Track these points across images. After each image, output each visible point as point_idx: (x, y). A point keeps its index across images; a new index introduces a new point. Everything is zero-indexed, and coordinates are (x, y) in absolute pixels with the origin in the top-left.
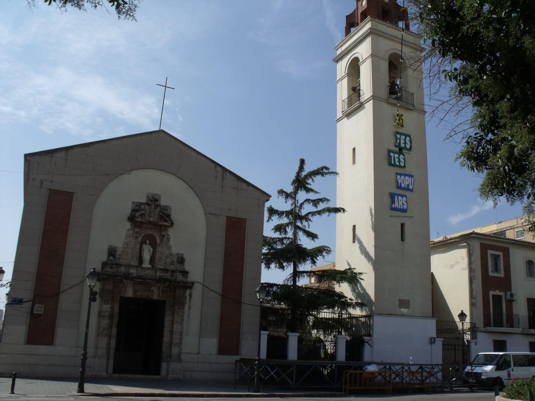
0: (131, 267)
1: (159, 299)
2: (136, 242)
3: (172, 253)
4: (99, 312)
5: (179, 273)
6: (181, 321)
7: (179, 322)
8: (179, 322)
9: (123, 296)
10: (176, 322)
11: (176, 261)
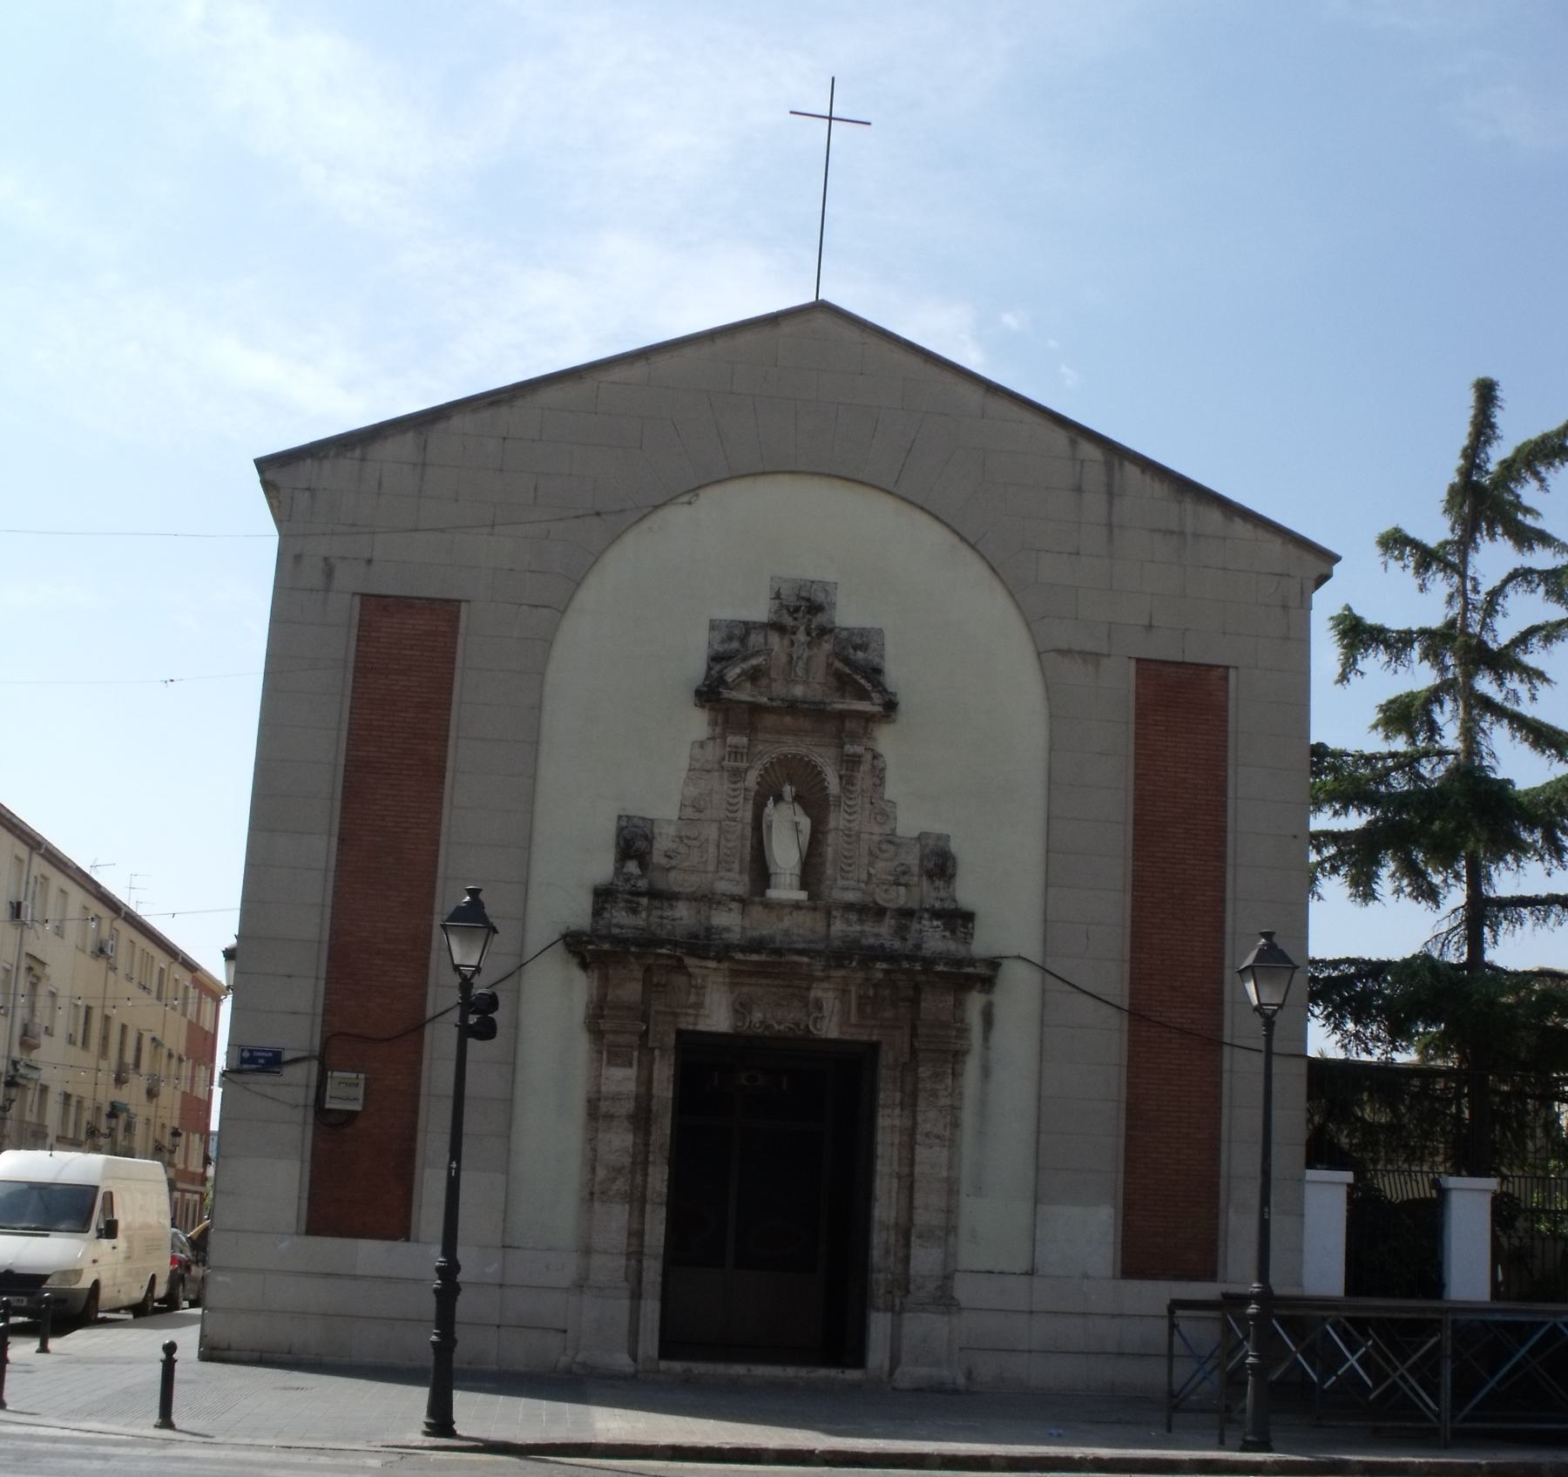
0: (719, 903)
1: (848, 1037)
2: (736, 793)
3: (899, 832)
4: (589, 1101)
5: (931, 920)
6: (947, 1134)
7: (938, 1137)
8: (938, 1137)
9: (691, 1027)
10: (927, 1135)
11: (915, 870)
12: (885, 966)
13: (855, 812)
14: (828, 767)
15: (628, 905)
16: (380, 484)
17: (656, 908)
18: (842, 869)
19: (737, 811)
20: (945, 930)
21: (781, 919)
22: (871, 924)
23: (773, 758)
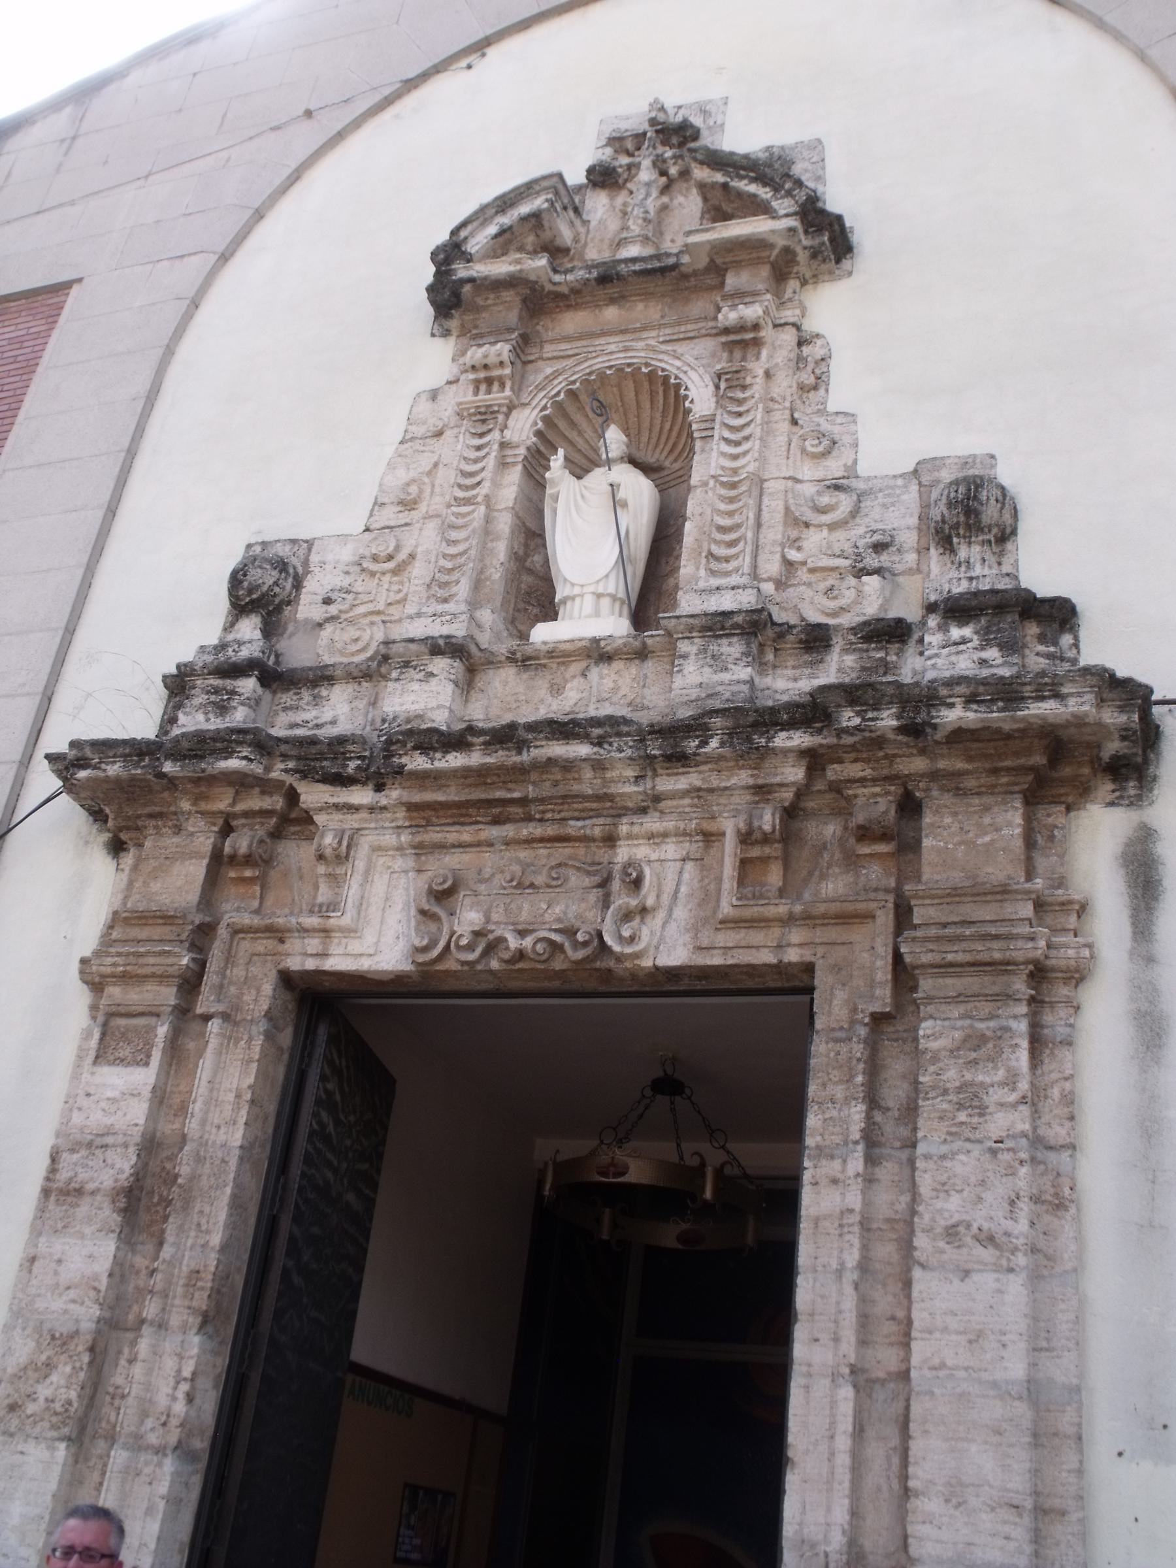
0: (406, 664)
1: (716, 960)
2: (481, 453)
3: (863, 469)
4: (51, 1156)
5: (943, 628)
6: (1023, 1226)
7: (988, 1240)
8: (988, 1240)
9: (311, 964)
10: (952, 1233)
11: (909, 538)
12: (799, 739)
13: (747, 438)
14: (692, 374)
15: (213, 698)
16: (9, 175)
17: (285, 709)
18: (710, 554)
19: (479, 483)
20: (985, 644)
21: (557, 690)
22: (790, 672)
23: (574, 382)
